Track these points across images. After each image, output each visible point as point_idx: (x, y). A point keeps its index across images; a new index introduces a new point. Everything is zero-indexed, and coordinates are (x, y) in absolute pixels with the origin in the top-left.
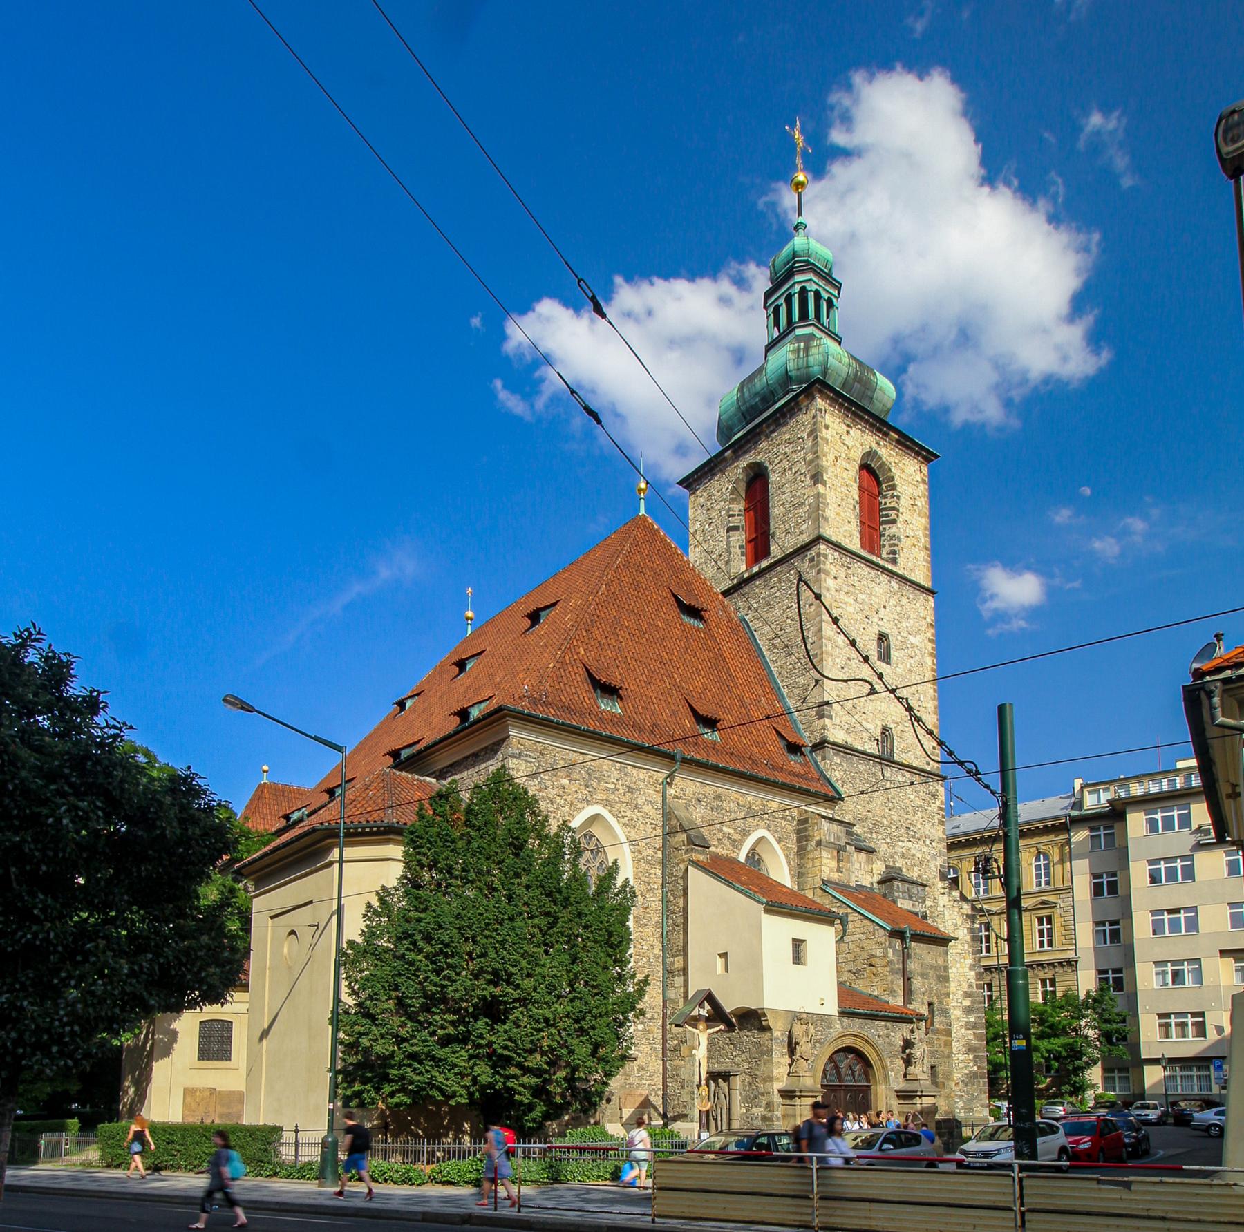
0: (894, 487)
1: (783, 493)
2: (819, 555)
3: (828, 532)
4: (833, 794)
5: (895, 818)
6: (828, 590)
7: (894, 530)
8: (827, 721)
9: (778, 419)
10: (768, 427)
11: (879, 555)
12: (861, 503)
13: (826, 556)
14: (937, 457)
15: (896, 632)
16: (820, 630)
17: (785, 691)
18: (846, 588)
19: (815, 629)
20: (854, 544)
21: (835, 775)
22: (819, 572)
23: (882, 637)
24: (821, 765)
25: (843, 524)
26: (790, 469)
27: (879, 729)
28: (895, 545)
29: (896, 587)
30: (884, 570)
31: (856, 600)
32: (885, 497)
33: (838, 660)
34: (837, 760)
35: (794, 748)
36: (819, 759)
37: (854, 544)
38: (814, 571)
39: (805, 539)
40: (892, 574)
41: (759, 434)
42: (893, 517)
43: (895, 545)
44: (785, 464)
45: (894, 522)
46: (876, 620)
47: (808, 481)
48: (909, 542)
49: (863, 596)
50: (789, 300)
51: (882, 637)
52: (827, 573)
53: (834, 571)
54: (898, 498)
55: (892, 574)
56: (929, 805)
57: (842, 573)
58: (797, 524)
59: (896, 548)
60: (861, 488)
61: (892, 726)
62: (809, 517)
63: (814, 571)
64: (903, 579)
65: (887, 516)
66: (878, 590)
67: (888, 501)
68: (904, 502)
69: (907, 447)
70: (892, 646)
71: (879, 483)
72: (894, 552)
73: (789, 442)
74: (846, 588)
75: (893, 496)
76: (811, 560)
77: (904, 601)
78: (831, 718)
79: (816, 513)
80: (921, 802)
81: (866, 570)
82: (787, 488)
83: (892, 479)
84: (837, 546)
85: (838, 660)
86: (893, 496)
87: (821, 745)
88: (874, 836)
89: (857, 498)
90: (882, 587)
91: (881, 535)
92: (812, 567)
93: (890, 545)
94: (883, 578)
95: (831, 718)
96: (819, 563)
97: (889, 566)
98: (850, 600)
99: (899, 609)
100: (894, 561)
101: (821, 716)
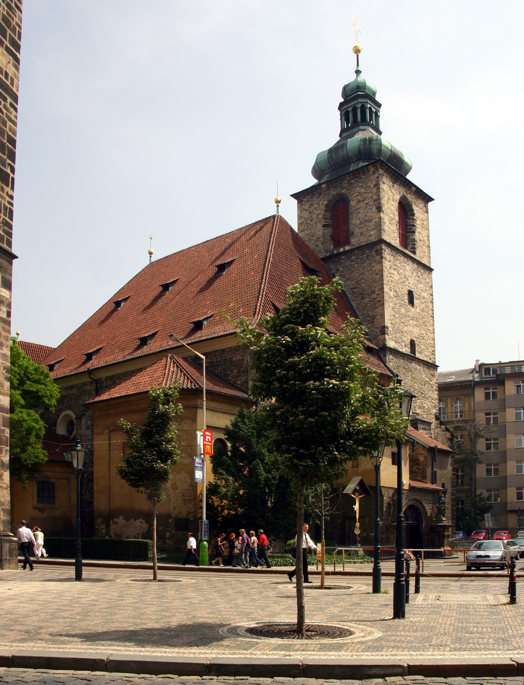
0: (413, 215)
1: (359, 213)
2: (381, 249)
3: (386, 237)
4: (392, 375)
6: (386, 268)
11: (406, 248)
12: (399, 222)
13: (385, 250)
16: (383, 288)
20: (396, 242)
21: (391, 365)
22: (382, 258)
23: (410, 294)
25: (391, 233)
26: (363, 201)
29: (416, 266)
32: (410, 219)
33: (391, 304)
34: (391, 357)
36: (382, 356)
37: (396, 242)
38: (378, 258)
39: (373, 239)
40: (414, 260)
44: (359, 197)
46: (407, 283)
47: (374, 208)
49: (401, 271)
50: (355, 109)
51: (410, 294)
52: (386, 259)
53: (388, 257)
54: (416, 220)
55: (414, 260)
57: (392, 259)
58: (367, 230)
60: (399, 214)
61: (415, 339)
62: (375, 229)
63: (378, 258)
65: (410, 229)
66: (408, 268)
67: (411, 221)
68: (418, 223)
70: (415, 298)
76: (377, 251)
77: (420, 274)
78: (388, 335)
79: (379, 226)
81: (402, 258)
82: (361, 211)
83: (413, 210)
84: (389, 245)
85: (391, 304)
89: (397, 219)
90: (409, 267)
92: (377, 255)
94: (410, 262)
95: (388, 335)
96: (381, 253)
97: (412, 255)
98: (396, 273)
100: (414, 253)
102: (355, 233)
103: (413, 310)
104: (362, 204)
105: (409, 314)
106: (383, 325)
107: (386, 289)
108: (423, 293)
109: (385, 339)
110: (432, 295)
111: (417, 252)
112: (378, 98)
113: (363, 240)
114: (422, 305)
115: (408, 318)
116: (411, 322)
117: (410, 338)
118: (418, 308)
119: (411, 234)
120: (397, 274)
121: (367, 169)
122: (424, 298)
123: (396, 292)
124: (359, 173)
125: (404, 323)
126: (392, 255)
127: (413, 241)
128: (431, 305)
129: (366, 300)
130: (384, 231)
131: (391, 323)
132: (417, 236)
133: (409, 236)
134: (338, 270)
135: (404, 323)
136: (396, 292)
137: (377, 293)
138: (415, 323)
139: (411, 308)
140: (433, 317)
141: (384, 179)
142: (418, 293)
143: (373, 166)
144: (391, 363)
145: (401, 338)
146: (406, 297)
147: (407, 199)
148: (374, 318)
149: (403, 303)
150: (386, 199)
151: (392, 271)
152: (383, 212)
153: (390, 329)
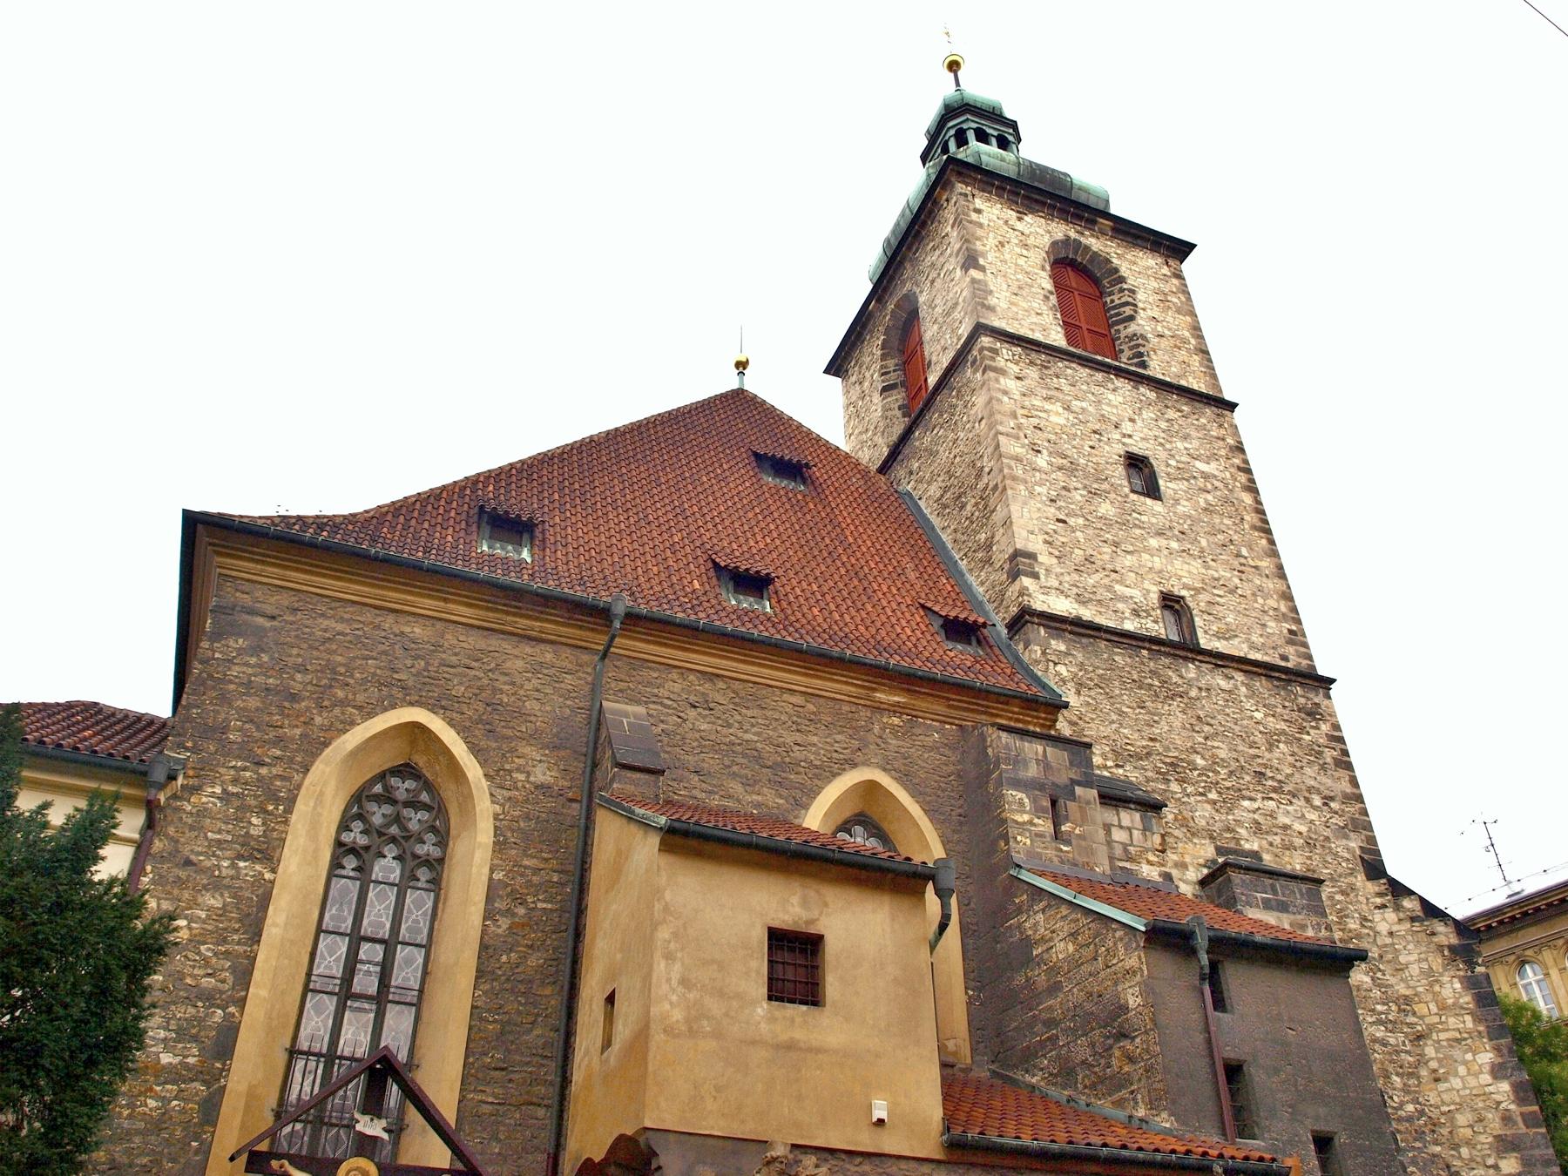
0: (1122, 280)
2: (982, 350)
5: (1223, 754)
6: (1005, 393)
7: (1133, 328)
8: (1026, 581)
9: (918, 232)
10: (909, 248)
14: (1192, 246)
15: (1163, 455)
17: (963, 564)
18: (1045, 393)
19: (990, 450)
24: (1026, 658)
27: (1154, 598)
28: (1138, 346)
29: (1152, 395)
30: (1120, 372)
31: (1068, 409)
32: (1111, 294)
34: (1058, 645)
35: (962, 630)
40: (1139, 379)
41: (901, 263)
42: (1128, 311)
43: (1138, 346)
45: (1131, 318)
46: (1118, 436)
47: (958, 272)
48: (1164, 343)
49: (1084, 404)
51: (1136, 463)
52: (1001, 372)
54: (1133, 292)
56: (1302, 730)
57: (1033, 373)
59: (1141, 349)
63: (979, 375)
64: (1163, 386)
65: (1119, 314)
67: (1115, 297)
69: (1138, 237)
71: (1096, 282)
72: (1141, 355)
73: (934, 249)
74: (1045, 393)
75: (1122, 290)
77: (1171, 414)
80: (1282, 726)
83: (1116, 270)
86: (1122, 290)
87: (1024, 619)
88: (1175, 787)
90: (1118, 397)
91: (1113, 341)
93: (1130, 349)
95: (1036, 576)
98: (1058, 407)
99: (1164, 425)
100: (1143, 365)
101: (1014, 575)
102: (934, 359)
103: (1157, 506)
104: (938, 283)
105: (1144, 518)
106: (1011, 551)
107: (1011, 447)
108: (1198, 464)
109: (1023, 592)
110: (1248, 471)
111: (1153, 364)
112: (1009, 114)
113: (945, 361)
114: (1210, 497)
115: (1138, 531)
116: (1154, 542)
117: (1155, 589)
118: (1184, 502)
119: (1121, 327)
120: (1061, 410)
121: (935, 203)
122: (1206, 476)
123: (1066, 457)
124: (924, 224)
125: (1116, 544)
126: (1032, 363)
127: (1131, 339)
128: (1248, 499)
129: (969, 507)
130: (991, 309)
131: (1046, 542)
132: (1142, 324)
133: (1118, 331)
134: (911, 473)
135: (1116, 544)
136: (1066, 457)
137: (987, 469)
138: (1174, 545)
139: (1149, 501)
140: (1268, 532)
141: (978, 203)
142: (1173, 463)
143: (944, 188)
144: (1061, 669)
145: (1109, 588)
146: (1119, 473)
147: (1087, 248)
148: (990, 546)
149: (1105, 486)
150: (991, 241)
151: (1037, 403)
152: (983, 269)
153: (1040, 558)
